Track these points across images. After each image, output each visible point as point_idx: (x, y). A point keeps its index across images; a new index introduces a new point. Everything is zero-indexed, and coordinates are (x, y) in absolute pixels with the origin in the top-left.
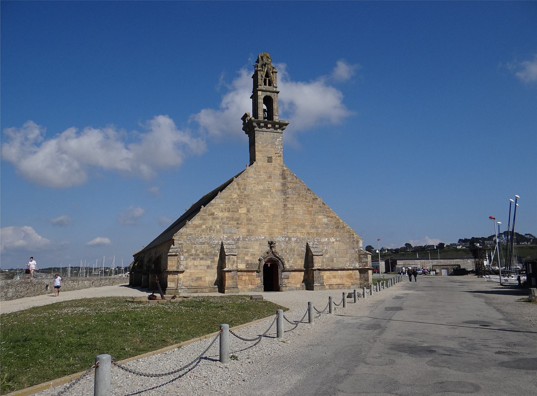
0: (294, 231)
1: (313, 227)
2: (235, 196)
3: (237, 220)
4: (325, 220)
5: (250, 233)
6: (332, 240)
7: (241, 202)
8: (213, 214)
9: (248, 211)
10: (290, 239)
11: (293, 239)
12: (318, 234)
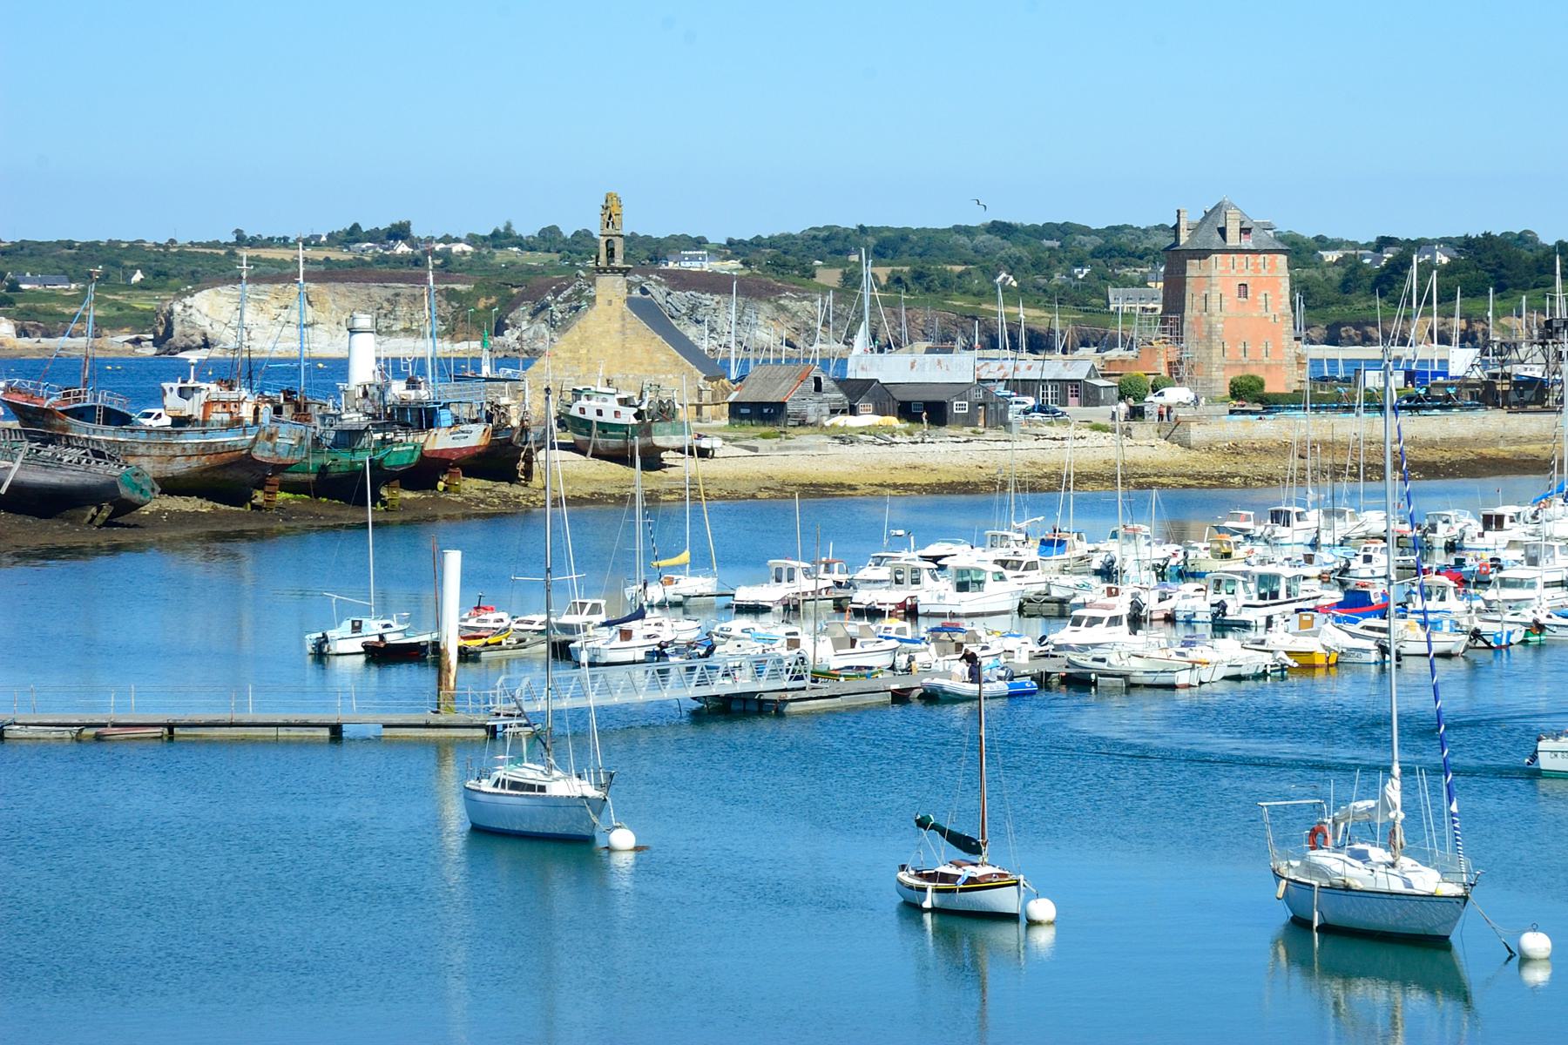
0: (632, 369)
1: (651, 364)
2: (576, 338)
3: (578, 359)
4: (664, 358)
5: (589, 371)
6: (670, 376)
7: (581, 344)
8: (556, 355)
9: (588, 351)
10: (627, 376)
11: (631, 376)
12: (655, 371)
